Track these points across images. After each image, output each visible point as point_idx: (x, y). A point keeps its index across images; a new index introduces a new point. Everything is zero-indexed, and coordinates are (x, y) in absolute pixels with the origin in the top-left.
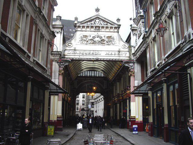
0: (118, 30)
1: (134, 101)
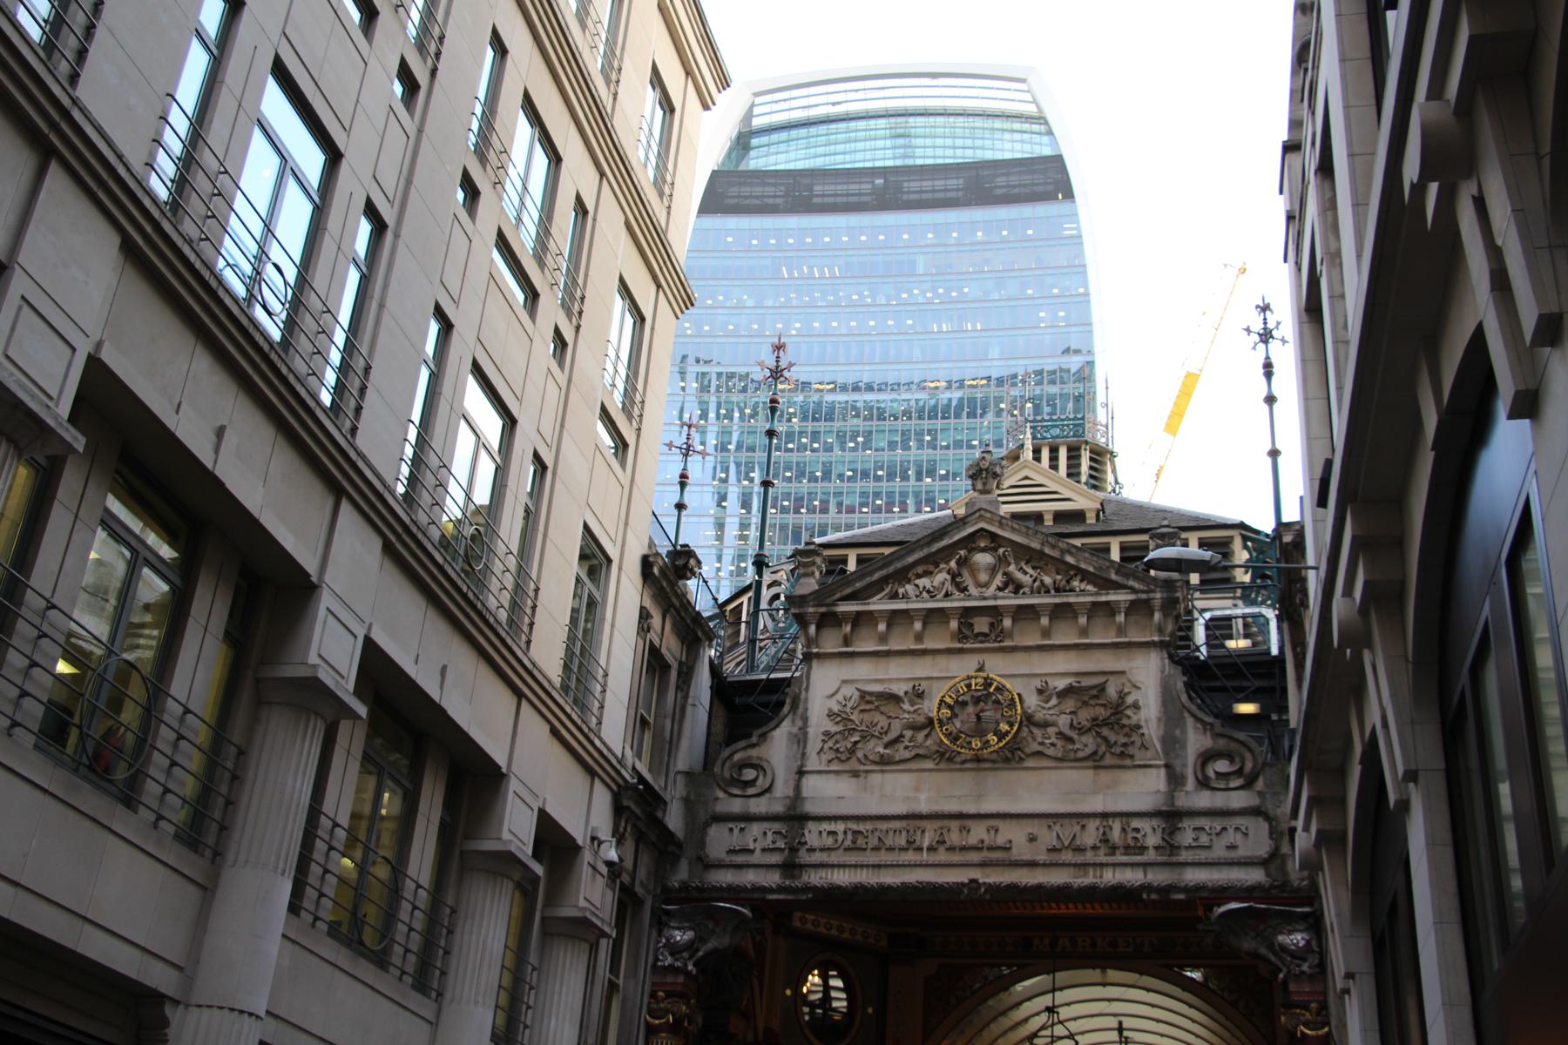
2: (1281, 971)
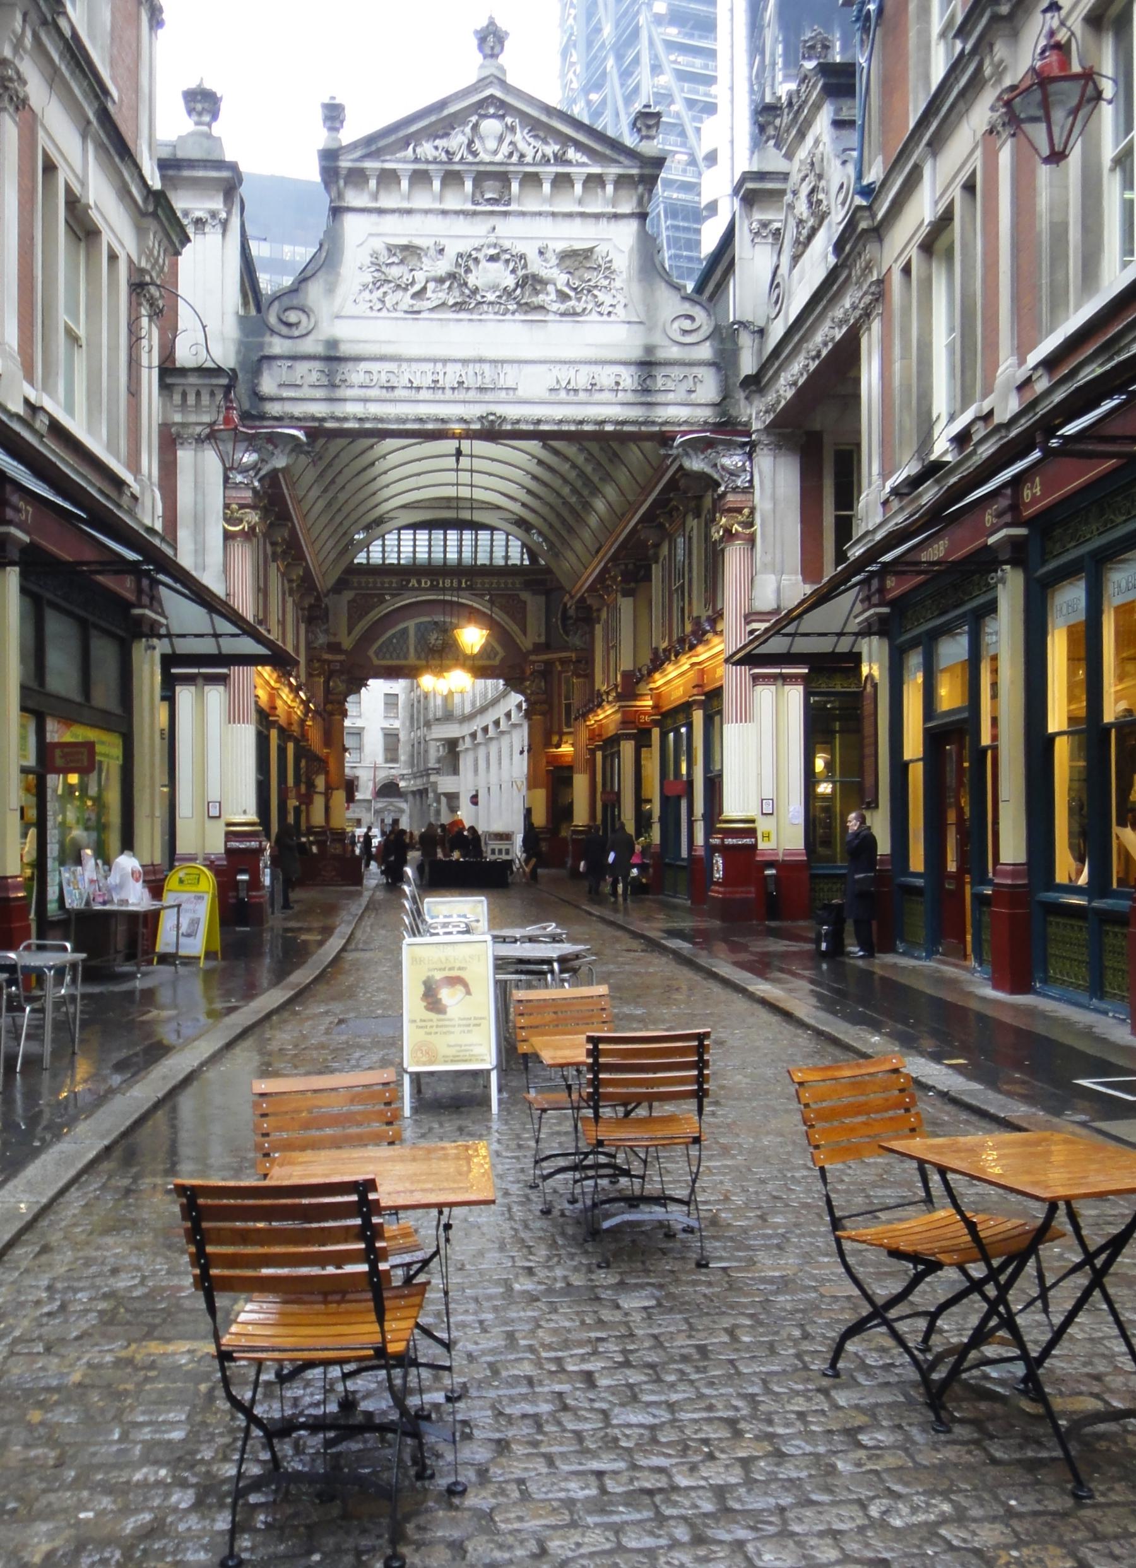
0: (640, 202)
1: (745, 716)
2: (719, 485)
